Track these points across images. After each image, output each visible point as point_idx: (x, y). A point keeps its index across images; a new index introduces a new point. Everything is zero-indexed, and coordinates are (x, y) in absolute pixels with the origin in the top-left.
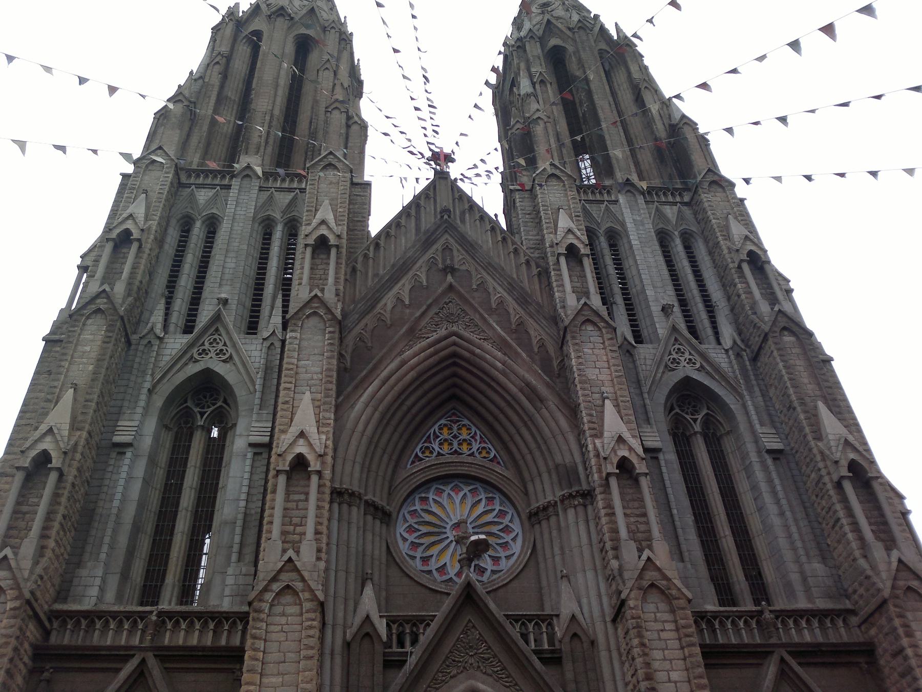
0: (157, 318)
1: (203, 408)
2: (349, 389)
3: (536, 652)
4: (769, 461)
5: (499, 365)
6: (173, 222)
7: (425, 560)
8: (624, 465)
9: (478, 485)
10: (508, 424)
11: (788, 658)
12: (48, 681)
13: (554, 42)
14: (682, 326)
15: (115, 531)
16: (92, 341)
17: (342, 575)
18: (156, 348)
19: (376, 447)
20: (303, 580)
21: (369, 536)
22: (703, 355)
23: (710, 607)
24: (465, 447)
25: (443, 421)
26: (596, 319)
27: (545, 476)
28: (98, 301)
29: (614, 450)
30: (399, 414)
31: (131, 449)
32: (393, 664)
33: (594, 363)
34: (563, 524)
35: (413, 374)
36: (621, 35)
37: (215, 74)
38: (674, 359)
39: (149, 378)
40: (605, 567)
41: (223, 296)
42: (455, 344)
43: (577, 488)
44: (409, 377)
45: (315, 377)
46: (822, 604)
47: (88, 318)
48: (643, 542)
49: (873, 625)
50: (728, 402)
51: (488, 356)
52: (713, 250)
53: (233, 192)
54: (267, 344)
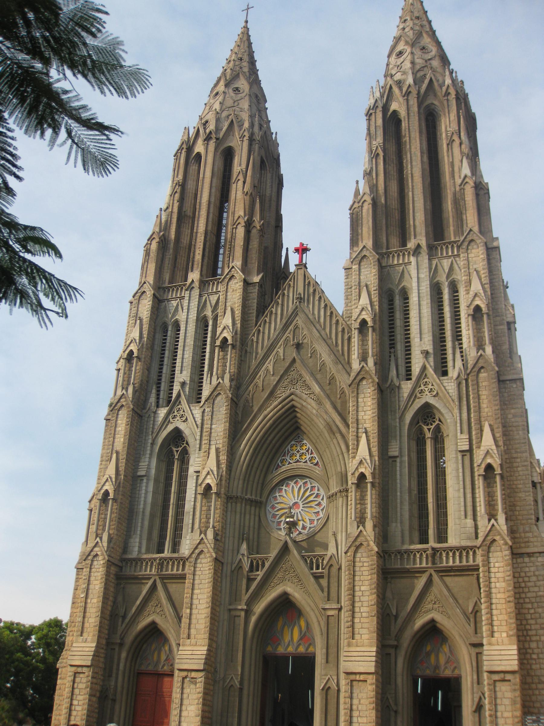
0: (152, 399)
1: (178, 447)
2: (239, 436)
3: (312, 574)
4: (460, 457)
5: (314, 411)
6: (158, 329)
11: (434, 574)
12: (124, 588)
13: (394, 106)
15: (143, 520)
17: (231, 538)
18: (152, 418)
19: (252, 467)
20: (207, 548)
21: (247, 517)
23: (406, 547)
24: (304, 457)
25: (293, 443)
26: (368, 377)
28: (122, 400)
29: (357, 469)
30: (265, 445)
31: (145, 478)
32: (250, 580)
37: (176, 202)
38: (422, 390)
39: (150, 437)
41: (182, 380)
42: (292, 400)
43: (344, 486)
46: (465, 543)
47: (119, 411)
48: (361, 521)
50: (447, 417)
53: (185, 303)
54: (202, 409)
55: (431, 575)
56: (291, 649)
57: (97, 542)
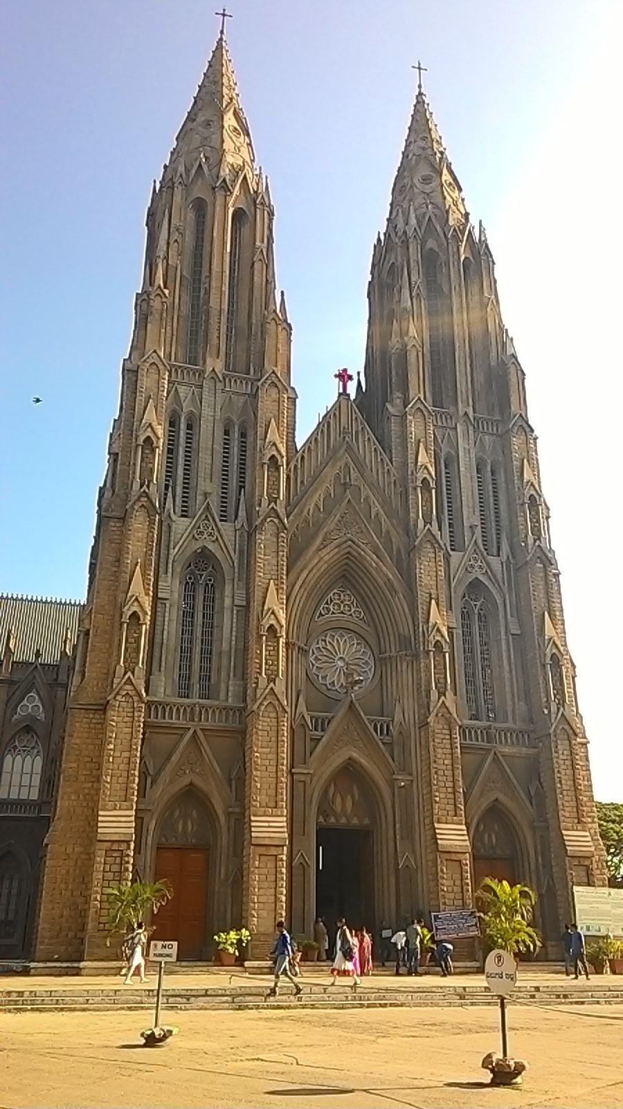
7: (324, 678)
8: (438, 645)
9: (353, 634)
10: (374, 601)
13: (431, 244)
14: (480, 541)
16: (142, 529)
22: (488, 564)
25: (335, 591)
33: (427, 572)
35: (326, 566)
36: (483, 239)
40: (418, 698)
41: (209, 490)
44: (323, 569)
45: (274, 568)
49: (541, 742)
51: (368, 557)
52: (510, 481)
55: (495, 753)
56: (343, 820)
57: (129, 678)
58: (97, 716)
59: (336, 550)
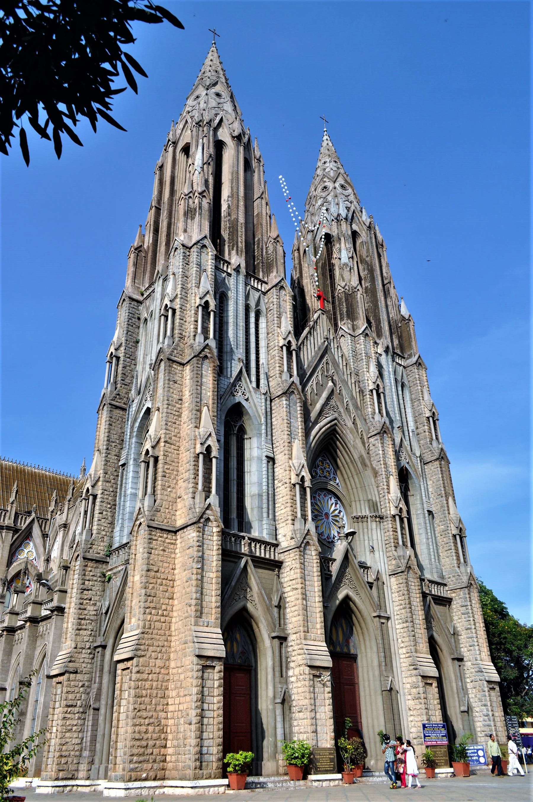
4: (427, 515)
25: (320, 459)
27: (362, 502)
28: (206, 350)
34: (370, 527)
42: (336, 424)
58: (169, 536)
59: (329, 425)
